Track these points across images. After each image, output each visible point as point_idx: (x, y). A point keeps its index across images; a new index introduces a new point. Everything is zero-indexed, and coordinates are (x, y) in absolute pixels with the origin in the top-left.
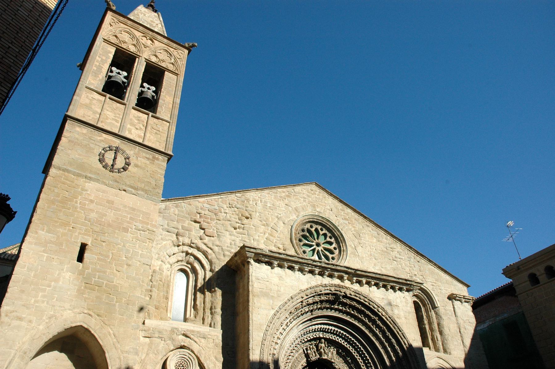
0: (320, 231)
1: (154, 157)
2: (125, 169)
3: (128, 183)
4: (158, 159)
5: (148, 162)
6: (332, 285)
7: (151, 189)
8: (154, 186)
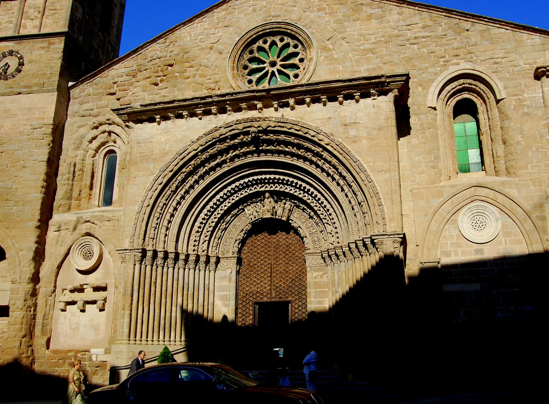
0: (264, 46)
1: (50, 44)
2: (19, 71)
3: (22, 84)
4: (53, 43)
5: (43, 52)
6: (238, 122)
7: (45, 81)
8: (49, 75)
